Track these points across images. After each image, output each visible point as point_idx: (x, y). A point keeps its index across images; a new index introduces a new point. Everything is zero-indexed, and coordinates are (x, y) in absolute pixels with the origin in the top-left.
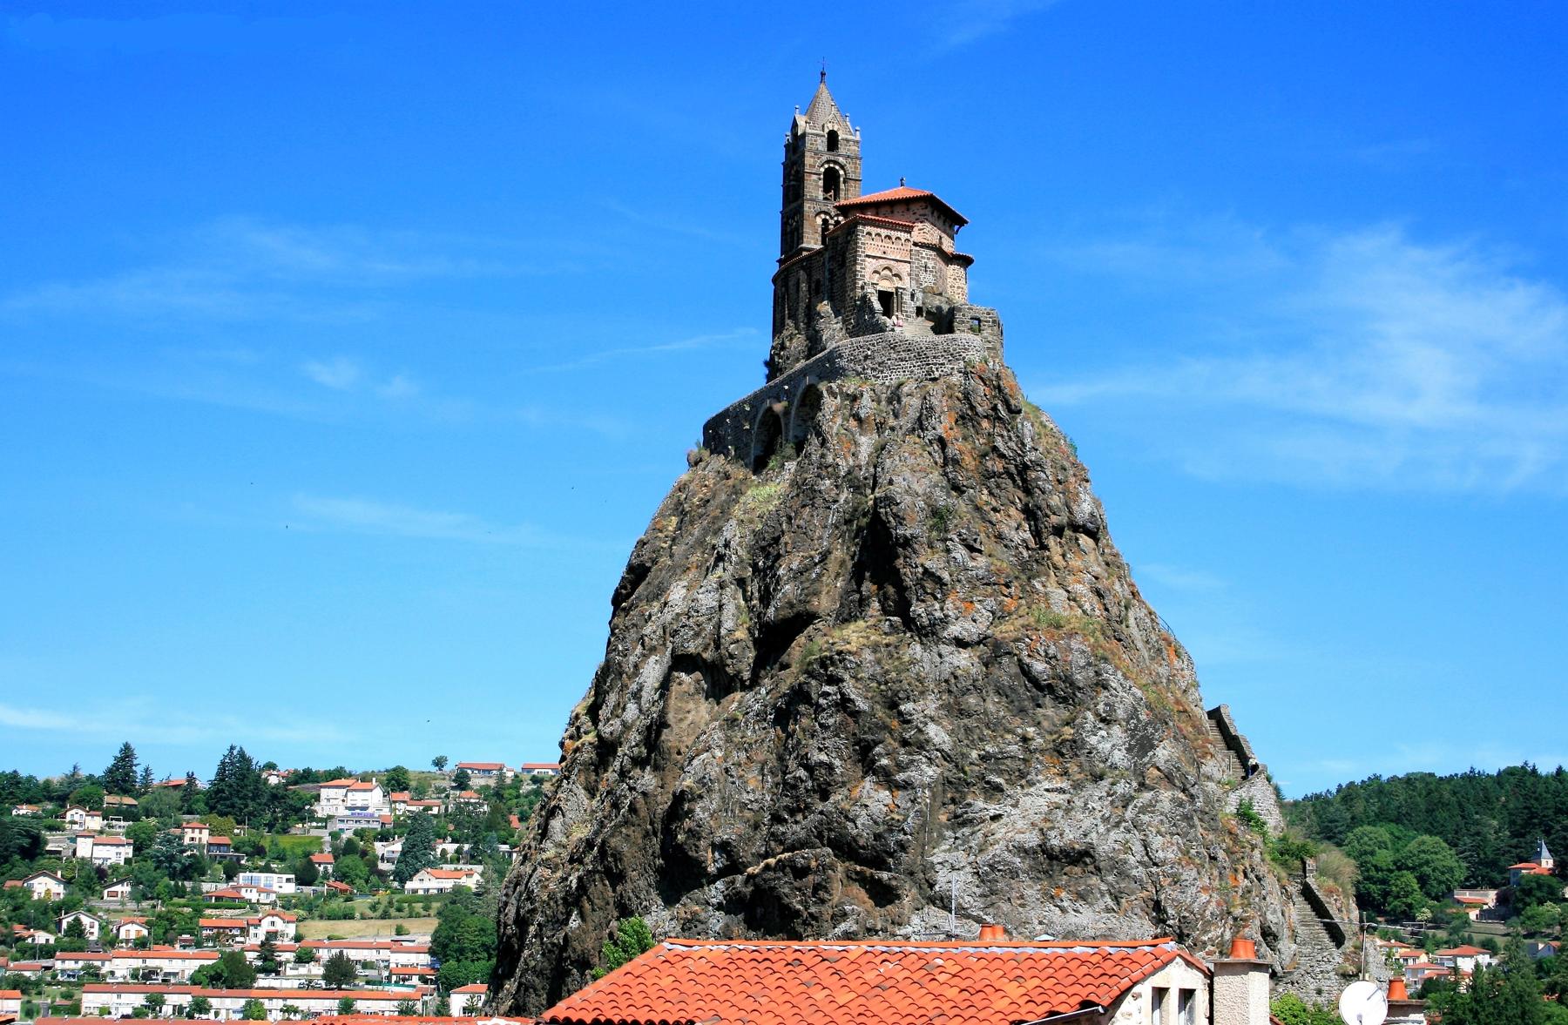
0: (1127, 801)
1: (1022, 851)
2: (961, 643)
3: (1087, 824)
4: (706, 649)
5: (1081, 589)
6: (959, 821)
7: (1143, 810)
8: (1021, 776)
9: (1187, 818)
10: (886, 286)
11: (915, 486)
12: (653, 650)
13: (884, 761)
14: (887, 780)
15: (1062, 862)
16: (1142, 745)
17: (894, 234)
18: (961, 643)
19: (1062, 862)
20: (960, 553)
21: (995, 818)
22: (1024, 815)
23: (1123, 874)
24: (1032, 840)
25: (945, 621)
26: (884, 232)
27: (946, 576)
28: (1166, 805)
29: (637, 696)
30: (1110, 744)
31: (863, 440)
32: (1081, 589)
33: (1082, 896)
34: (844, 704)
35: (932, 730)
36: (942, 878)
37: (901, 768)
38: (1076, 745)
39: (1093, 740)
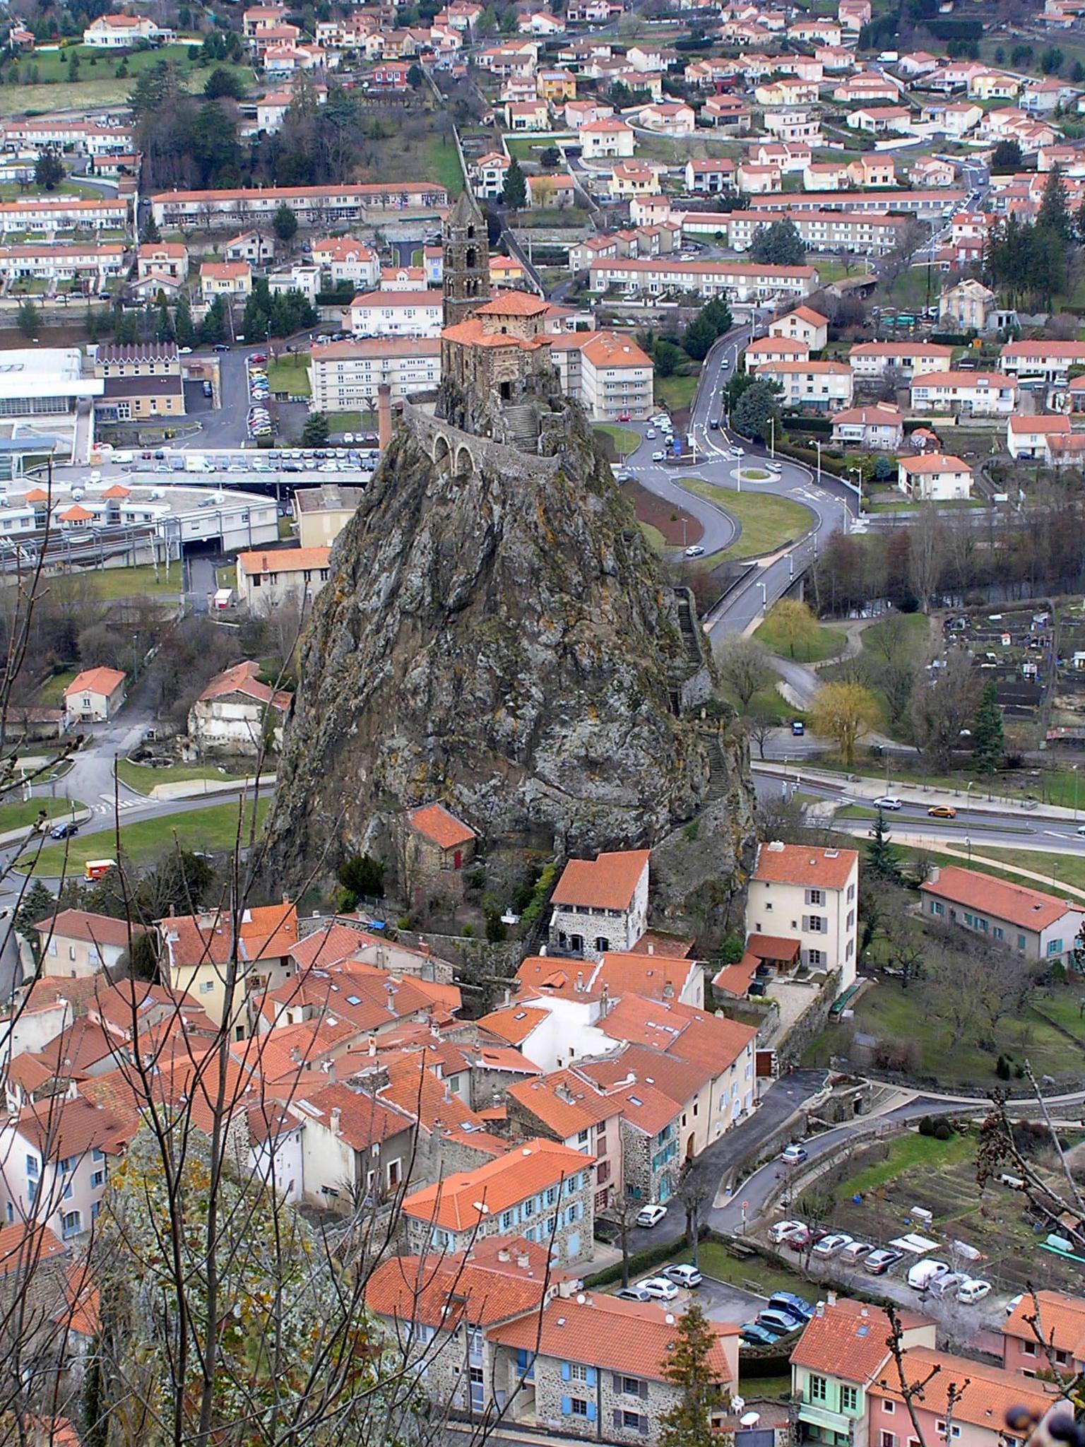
0: (626, 734)
1: (578, 758)
2: (547, 646)
3: (608, 745)
4: (418, 609)
5: (608, 607)
6: (548, 736)
7: (634, 737)
8: (576, 715)
9: (656, 739)
10: (505, 379)
11: (523, 552)
12: (385, 570)
13: (511, 704)
14: (512, 712)
15: (593, 766)
16: (635, 704)
17: (508, 349)
18: (547, 646)
19: (593, 766)
20: (545, 595)
21: (565, 737)
22: (578, 734)
23: (624, 770)
24: (583, 752)
25: (540, 633)
26: (503, 350)
27: (539, 609)
28: (645, 734)
29: (378, 594)
30: (619, 703)
31: (495, 507)
32: (608, 607)
33: (605, 779)
34: (489, 669)
35: (534, 690)
36: (540, 764)
37: (519, 708)
38: (604, 704)
39: (611, 701)
